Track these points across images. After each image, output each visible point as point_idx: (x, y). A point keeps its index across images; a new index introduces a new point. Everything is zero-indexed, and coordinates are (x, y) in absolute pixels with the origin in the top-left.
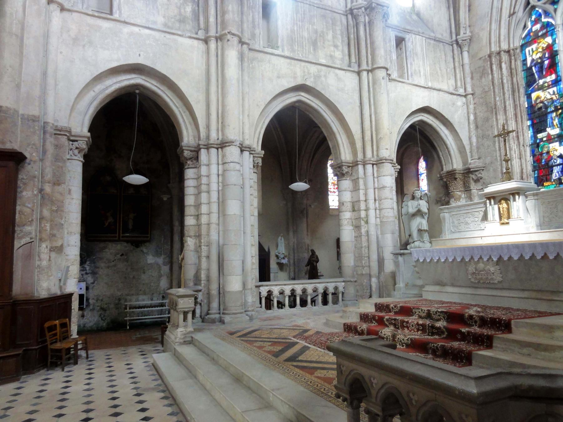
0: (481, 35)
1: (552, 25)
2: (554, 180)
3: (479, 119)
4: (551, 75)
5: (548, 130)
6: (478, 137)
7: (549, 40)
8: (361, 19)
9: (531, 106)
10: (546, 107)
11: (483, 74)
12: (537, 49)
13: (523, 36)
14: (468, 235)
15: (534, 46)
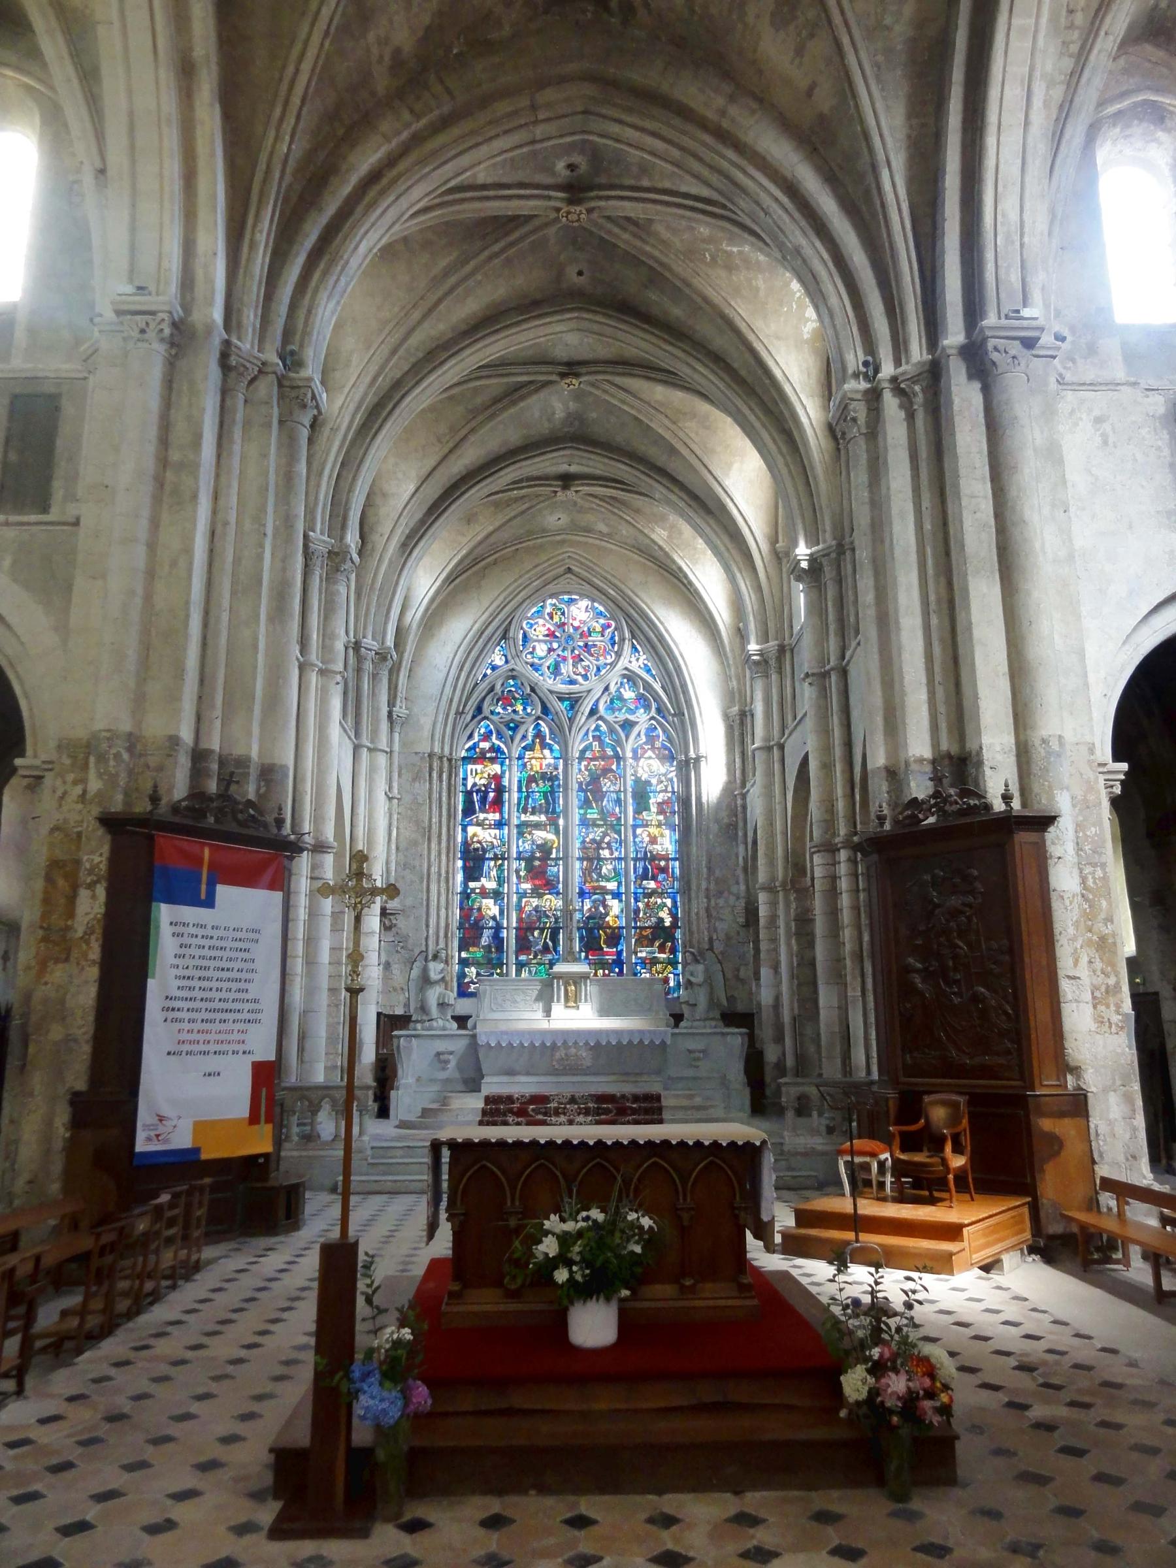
0: (422, 722)
1: (503, 753)
2: (483, 947)
3: (401, 838)
4: (494, 812)
5: (483, 880)
6: (397, 864)
7: (496, 768)
8: (368, 666)
9: (466, 843)
10: (484, 851)
11: (416, 778)
12: (482, 773)
13: (467, 746)
14: (515, 1016)
15: (479, 767)
